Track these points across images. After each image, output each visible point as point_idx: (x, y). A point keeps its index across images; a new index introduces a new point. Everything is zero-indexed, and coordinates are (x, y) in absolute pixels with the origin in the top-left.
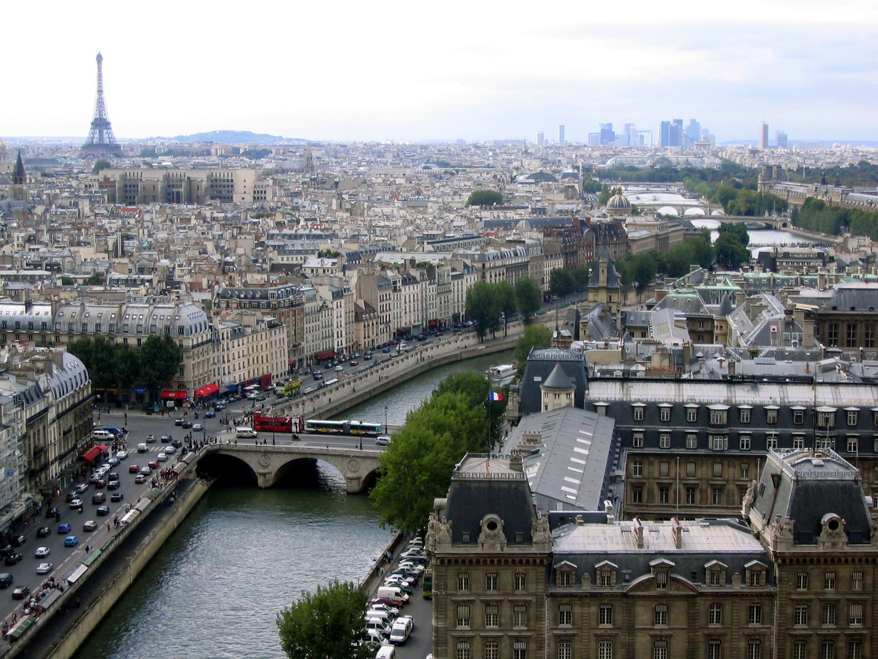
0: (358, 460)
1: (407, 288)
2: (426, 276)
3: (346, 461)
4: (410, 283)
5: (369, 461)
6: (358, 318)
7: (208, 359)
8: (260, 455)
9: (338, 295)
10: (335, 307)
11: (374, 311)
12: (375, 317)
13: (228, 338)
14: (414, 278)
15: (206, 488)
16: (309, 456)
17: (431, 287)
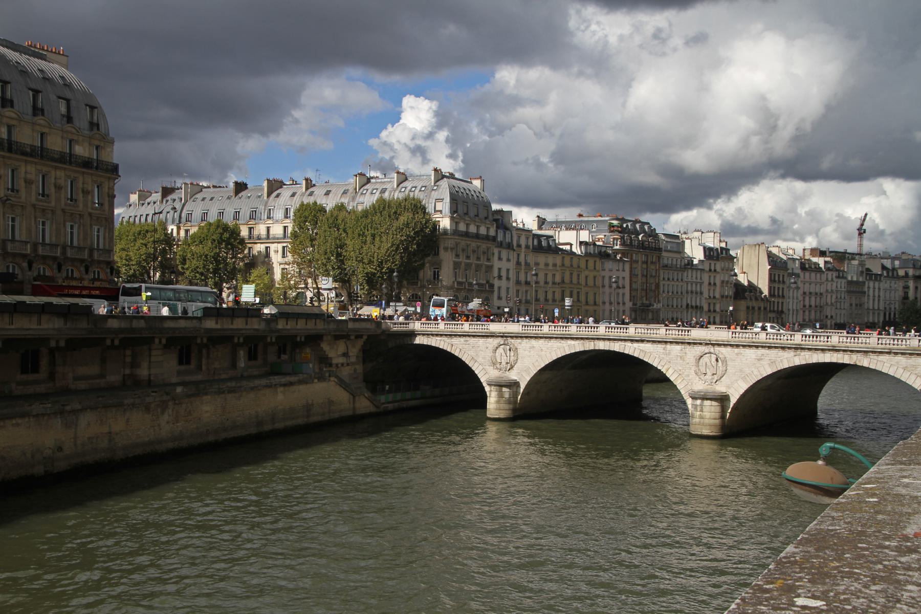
5: (751, 353)
10: (707, 269)
11: (761, 293)
13: (527, 247)
14: (816, 264)
16: (602, 346)
17: (839, 280)
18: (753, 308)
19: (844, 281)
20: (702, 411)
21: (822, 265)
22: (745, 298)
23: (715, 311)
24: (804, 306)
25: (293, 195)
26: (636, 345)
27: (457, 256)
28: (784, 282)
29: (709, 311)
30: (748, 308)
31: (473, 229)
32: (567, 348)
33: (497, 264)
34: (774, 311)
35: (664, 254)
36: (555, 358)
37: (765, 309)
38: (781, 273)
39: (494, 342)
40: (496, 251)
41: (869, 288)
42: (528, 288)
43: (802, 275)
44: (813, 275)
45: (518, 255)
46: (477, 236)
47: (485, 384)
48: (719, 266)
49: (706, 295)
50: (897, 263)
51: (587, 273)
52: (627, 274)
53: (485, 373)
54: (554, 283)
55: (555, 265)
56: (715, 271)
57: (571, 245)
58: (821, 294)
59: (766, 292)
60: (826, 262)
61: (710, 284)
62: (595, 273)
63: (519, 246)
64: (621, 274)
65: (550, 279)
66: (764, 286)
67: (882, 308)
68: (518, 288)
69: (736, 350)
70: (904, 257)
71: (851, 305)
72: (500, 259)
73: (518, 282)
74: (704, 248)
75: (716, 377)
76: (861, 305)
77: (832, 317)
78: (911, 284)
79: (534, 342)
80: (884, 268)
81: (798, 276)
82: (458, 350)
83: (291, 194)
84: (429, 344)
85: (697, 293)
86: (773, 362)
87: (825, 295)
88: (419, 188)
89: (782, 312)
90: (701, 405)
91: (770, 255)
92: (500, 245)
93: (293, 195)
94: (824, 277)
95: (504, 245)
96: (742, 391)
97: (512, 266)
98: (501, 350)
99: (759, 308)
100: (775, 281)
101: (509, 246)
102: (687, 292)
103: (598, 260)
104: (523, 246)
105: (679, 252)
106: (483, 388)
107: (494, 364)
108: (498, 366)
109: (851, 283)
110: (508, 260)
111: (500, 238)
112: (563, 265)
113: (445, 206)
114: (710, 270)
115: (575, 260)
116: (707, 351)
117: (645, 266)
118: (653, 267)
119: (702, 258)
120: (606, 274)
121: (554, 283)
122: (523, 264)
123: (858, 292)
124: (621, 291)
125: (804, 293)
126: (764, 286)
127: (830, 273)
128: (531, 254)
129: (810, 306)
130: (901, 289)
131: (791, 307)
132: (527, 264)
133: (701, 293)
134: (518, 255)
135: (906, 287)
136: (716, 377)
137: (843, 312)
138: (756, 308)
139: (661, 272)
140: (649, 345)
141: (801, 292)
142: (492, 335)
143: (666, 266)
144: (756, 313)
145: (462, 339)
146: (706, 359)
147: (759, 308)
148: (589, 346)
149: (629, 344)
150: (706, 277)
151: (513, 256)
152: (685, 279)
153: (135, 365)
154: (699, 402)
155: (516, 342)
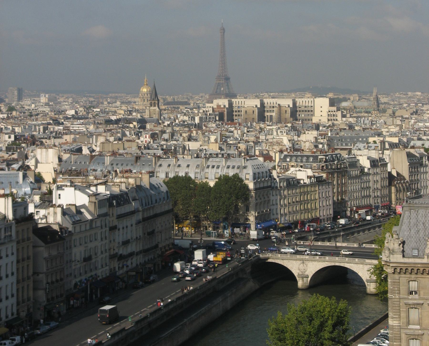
7: (269, 201)
9: (374, 163)
11: (404, 179)
15: (257, 287)
16: (337, 264)
25: (169, 165)
26: (348, 264)
46: (264, 188)
47: (296, 276)
53: (295, 272)
83: (168, 165)
93: (169, 165)
106: (296, 278)
107: (299, 269)
113: (250, 176)
119: (369, 167)
126: (406, 173)
140: (352, 264)
145: (287, 261)
149: (346, 264)
154: (369, 283)
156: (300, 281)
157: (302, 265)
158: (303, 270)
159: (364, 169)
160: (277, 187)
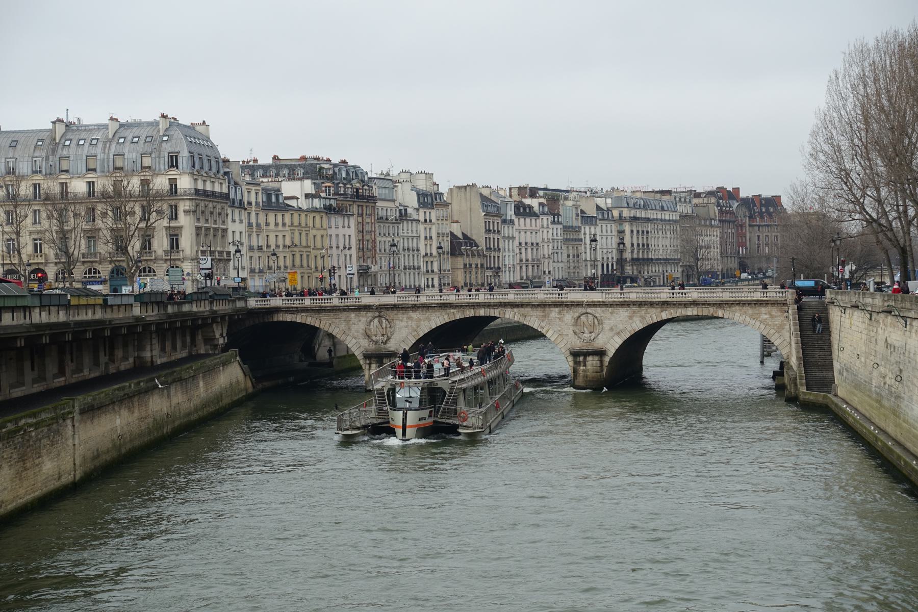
0: (598, 312)
1: (522, 220)
2: (546, 209)
3: (569, 316)
4: (525, 214)
5: (623, 313)
6: (455, 251)
7: (225, 231)
8: (370, 315)
10: (422, 220)
11: (477, 246)
12: (479, 255)
14: (530, 207)
16: (482, 312)
17: (555, 226)
18: (471, 265)
19: (560, 226)
20: (585, 365)
21: (536, 209)
22: (462, 254)
23: (433, 271)
24: (521, 261)
27: (198, 219)
28: (499, 231)
29: (427, 271)
30: (465, 265)
31: (209, 187)
32: (446, 317)
33: (231, 227)
34: (491, 268)
35: (379, 204)
36: (434, 327)
37: (482, 265)
38: (496, 220)
39: (365, 317)
40: (229, 211)
41: (585, 234)
42: (260, 254)
43: (516, 221)
44: (528, 220)
45: (249, 214)
46: (212, 194)
48: (434, 214)
49: (422, 252)
50: (609, 201)
51: (313, 232)
52: (352, 231)
54: (284, 247)
55: (284, 225)
56: (430, 221)
57: (298, 198)
58: (537, 244)
59: (482, 246)
60: (540, 204)
61: (426, 238)
62: (322, 232)
63: (250, 203)
64: (347, 232)
65: (280, 243)
66: (479, 236)
67: (599, 258)
68: (252, 254)
69: (610, 309)
70: (615, 194)
71: (568, 256)
72: (234, 221)
73: (251, 248)
74: (418, 195)
75: (593, 335)
76: (578, 256)
77: (549, 272)
78: (627, 228)
79: (411, 313)
80: (598, 208)
81: (512, 222)
82: (327, 325)
84: (294, 320)
85: (413, 250)
86: (643, 318)
87: (541, 245)
88: (129, 138)
89: (499, 268)
90: (585, 361)
91: (484, 198)
92: (233, 205)
94: (539, 221)
95: (236, 204)
96: (617, 346)
97: (243, 227)
98: (376, 321)
99: (477, 265)
100: (490, 231)
101: (241, 205)
102: (404, 250)
103: (324, 215)
104: (254, 204)
105: (394, 201)
107: (368, 336)
108: (374, 338)
109: (566, 229)
110: (241, 221)
111: (232, 196)
112: (292, 224)
114: (426, 221)
115: (303, 215)
116: (584, 311)
117: (360, 219)
118: (368, 220)
119: (416, 205)
120: (333, 231)
121: (284, 247)
122: (254, 225)
123: (576, 240)
124: (347, 252)
125: (520, 244)
127: (545, 218)
128: (261, 213)
129: (527, 260)
130: (615, 233)
131: (507, 263)
132: (258, 225)
133: (418, 250)
134: (249, 214)
135: (621, 232)
136: (593, 335)
137: (561, 265)
138: (474, 266)
139: (377, 225)
141: (516, 242)
142: (367, 308)
143: (382, 218)
144: (474, 271)
146: (583, 318)
147: (477, 265)
148: (470, 313)
149: (508, 310)
150: (422, 227)
151: (244, 214)
152: (401, 234)
153: (141, 348)
154: (581, 359)
155: (391, 315)
156: (373, 366)
157: (376, 321)
158: (379, 338)
159: (406, 210)
160: (241, 202)
